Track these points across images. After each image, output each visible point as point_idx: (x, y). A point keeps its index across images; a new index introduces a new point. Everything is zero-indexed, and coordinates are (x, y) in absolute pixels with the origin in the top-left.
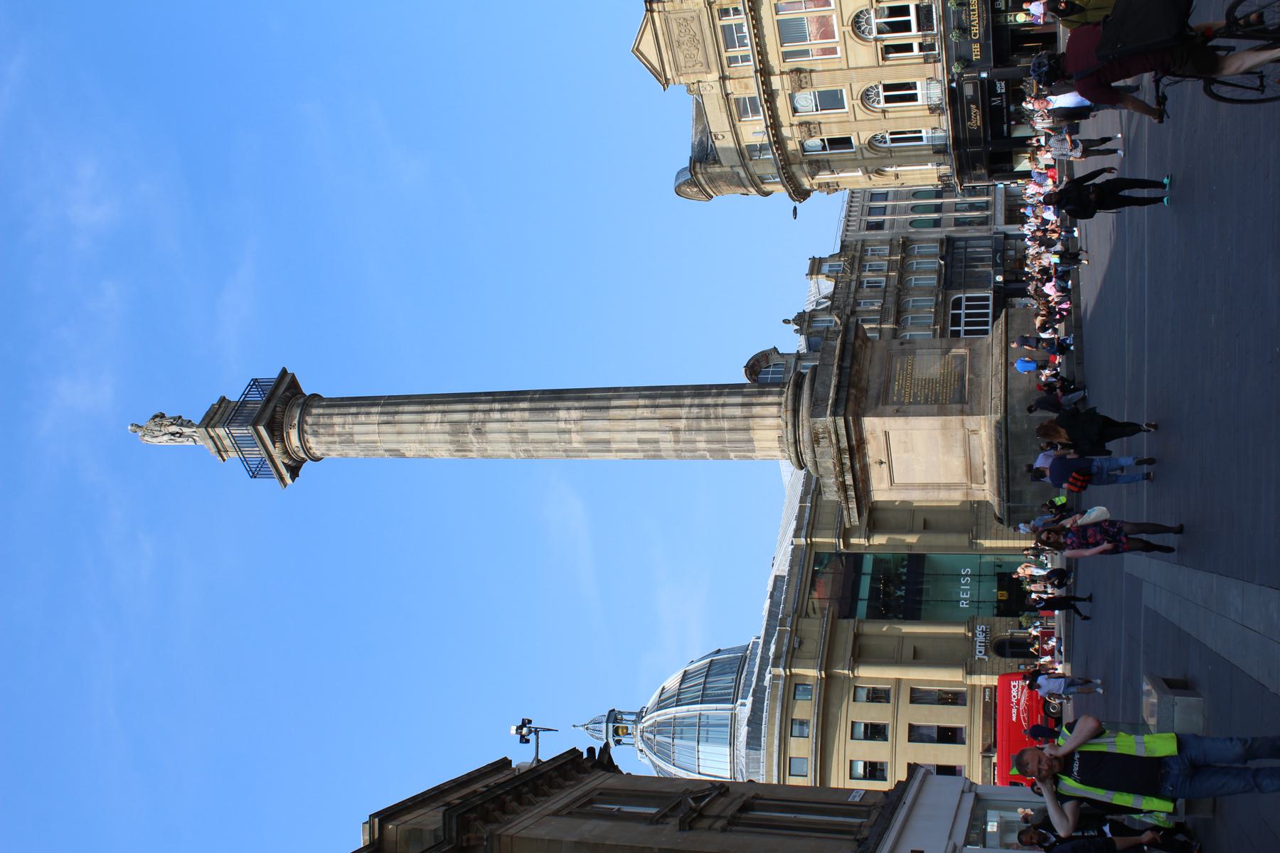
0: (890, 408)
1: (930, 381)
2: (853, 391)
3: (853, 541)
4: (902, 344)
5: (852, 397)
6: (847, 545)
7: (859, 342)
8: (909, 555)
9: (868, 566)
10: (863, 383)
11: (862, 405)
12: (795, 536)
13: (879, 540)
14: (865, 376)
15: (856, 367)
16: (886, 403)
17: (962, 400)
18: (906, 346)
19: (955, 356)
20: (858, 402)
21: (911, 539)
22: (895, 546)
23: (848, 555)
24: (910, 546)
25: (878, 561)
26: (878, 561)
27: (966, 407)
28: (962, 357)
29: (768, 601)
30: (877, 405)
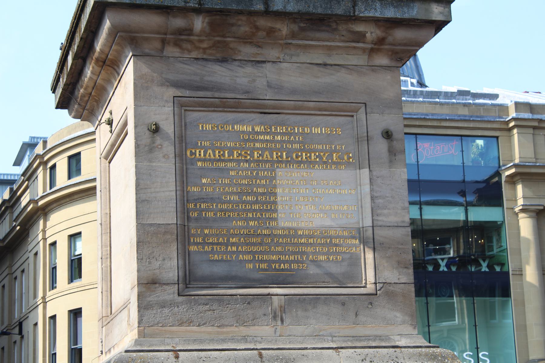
0: (165, 115)
1: (268, 204)
2: (199, 23)
3: (520, 188)
4: (387, 135)
5: (178, 22)
6: (513, 180)
7: (372, 33)
8: (508, 273)
9: (482, 214)
10: (248, 51)
11: (171, 51)
12: (517, 104)
13: (526, 226)
14: (273, 53)
15: (284, 28)
16: (182, 106)
17: (189, 281)
18: (381, 146)
19: (355, 262)
20: (181, 38)
21: (531, 274)
22: (518, 252)
23: (499, 184)
24: (520, 273)
25: (490, 231)
26: (490, 231)
27: (170, 293)
28: (352, 276)
29: (455, 90)
30: (176, 85)
